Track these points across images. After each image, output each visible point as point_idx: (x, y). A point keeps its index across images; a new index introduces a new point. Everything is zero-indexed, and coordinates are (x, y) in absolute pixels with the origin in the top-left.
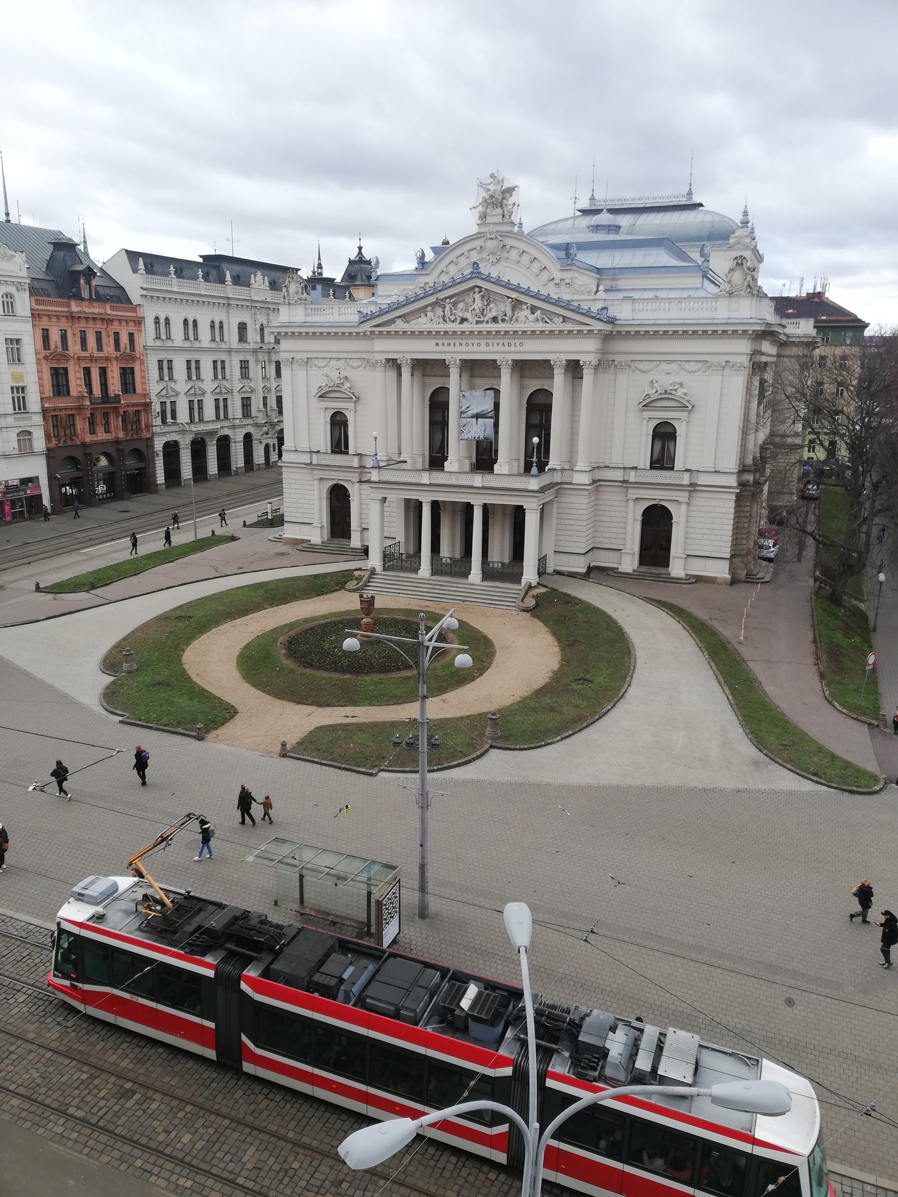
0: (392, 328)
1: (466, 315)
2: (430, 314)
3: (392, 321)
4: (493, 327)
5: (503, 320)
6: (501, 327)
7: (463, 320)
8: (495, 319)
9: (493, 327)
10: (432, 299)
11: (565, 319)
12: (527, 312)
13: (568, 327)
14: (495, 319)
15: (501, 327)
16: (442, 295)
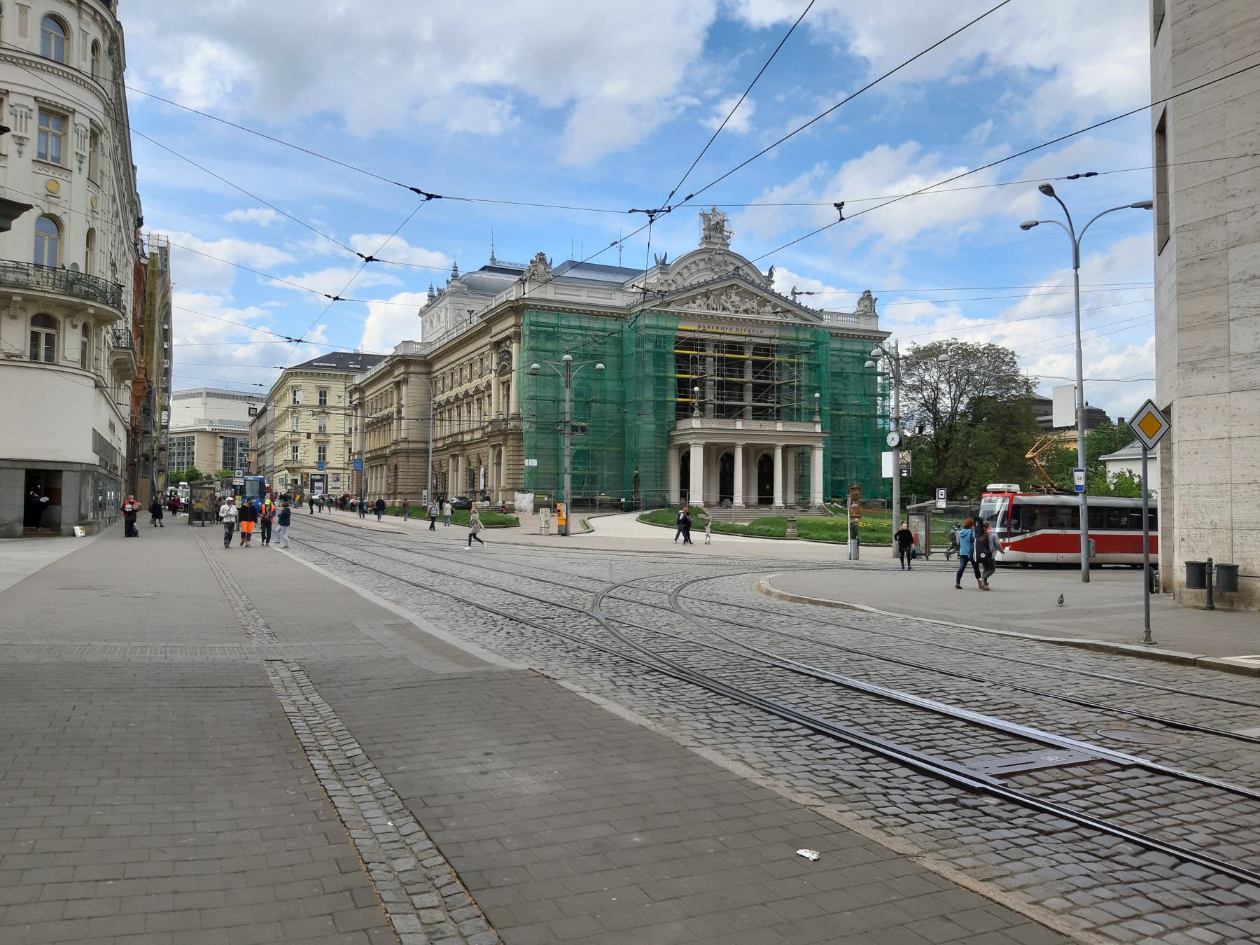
0: (670, 309)
1: (728, 305)
2: (698, 302)
3: (669, 304)
4: (745, 316)
5: (752, 312)
6: (751, 316)
7: (724, 309)
8: (746, 311)
9: (745, 316)
10: (703, 290)
11: (796, 316)
12: (770, 308)
13: (798, 321)
14: (746, 311)
15: (751, 316)
16: (712, 288)
